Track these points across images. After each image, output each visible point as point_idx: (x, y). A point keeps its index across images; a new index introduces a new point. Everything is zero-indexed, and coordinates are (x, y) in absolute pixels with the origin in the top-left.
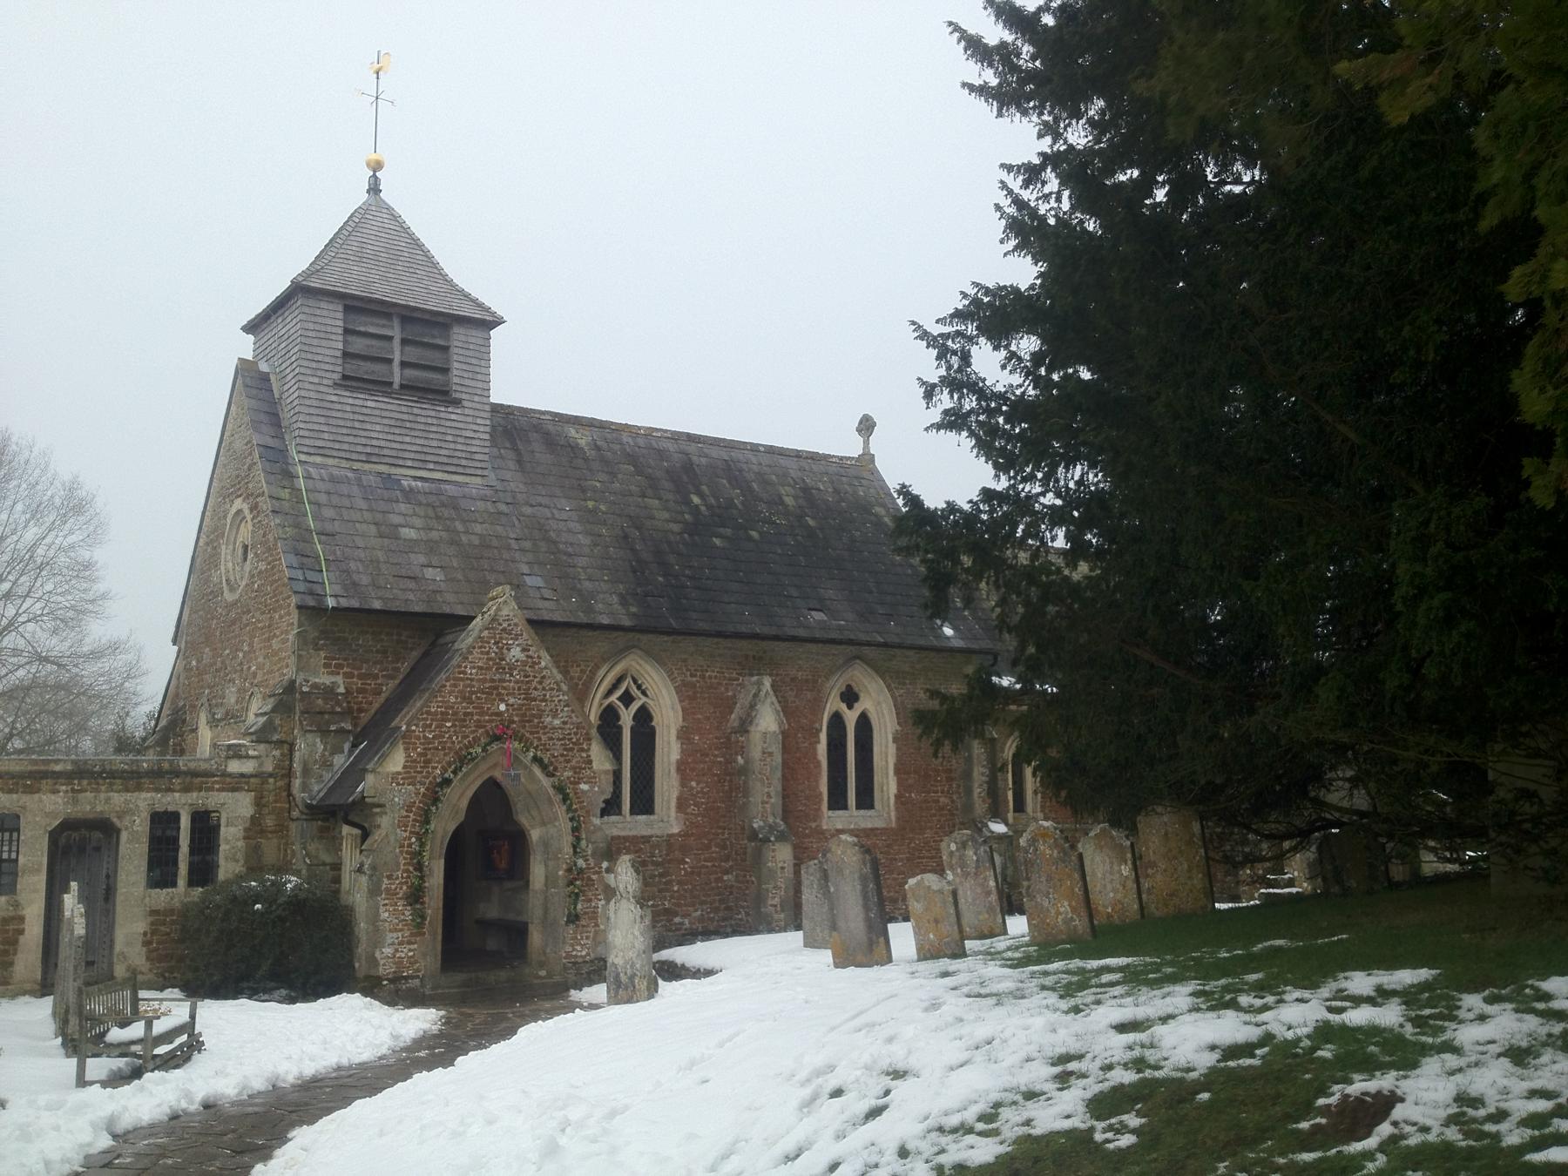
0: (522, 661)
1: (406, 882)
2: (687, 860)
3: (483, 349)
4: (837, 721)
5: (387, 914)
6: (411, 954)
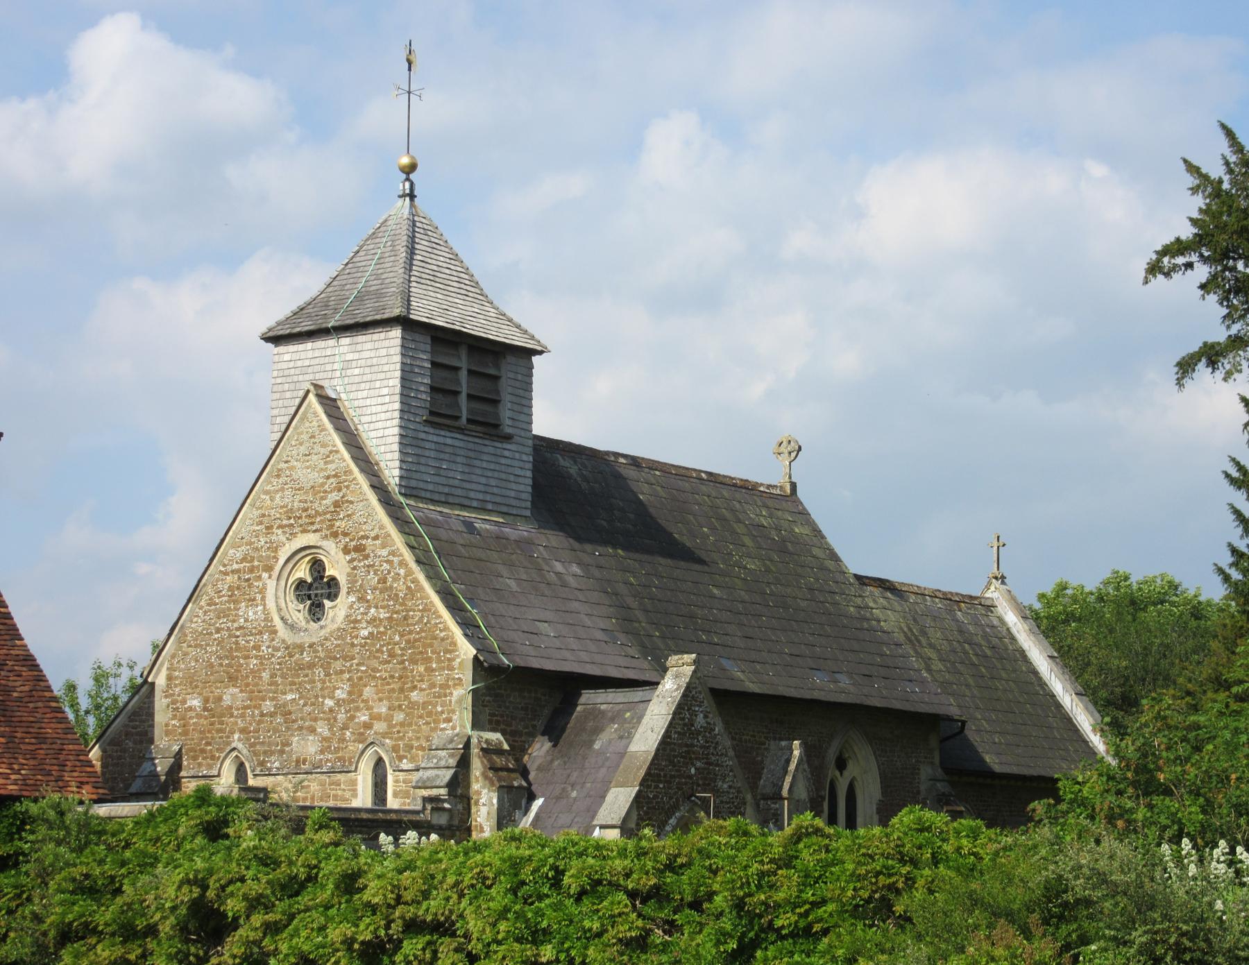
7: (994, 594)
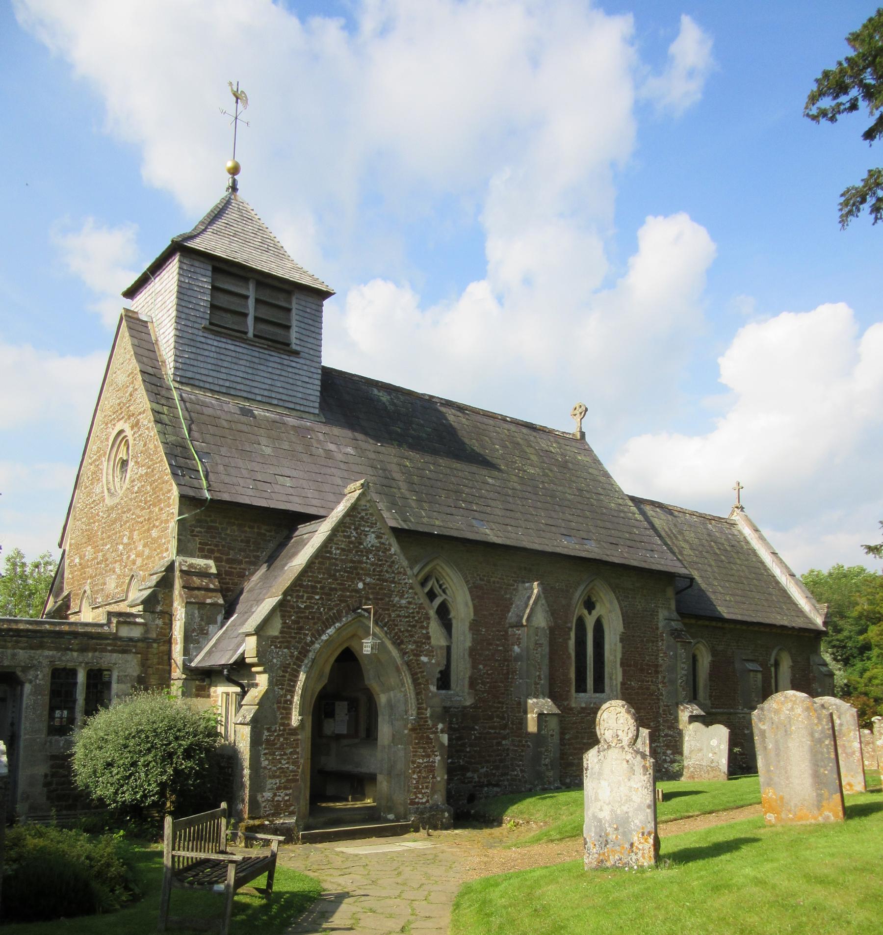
0: (377, 547)
1: (282, 735)
2: (477, 727)
3: (317, 313)
4: (581, 624)
5: (267, 762)
6: (287, 798)
7: (737, 517)
